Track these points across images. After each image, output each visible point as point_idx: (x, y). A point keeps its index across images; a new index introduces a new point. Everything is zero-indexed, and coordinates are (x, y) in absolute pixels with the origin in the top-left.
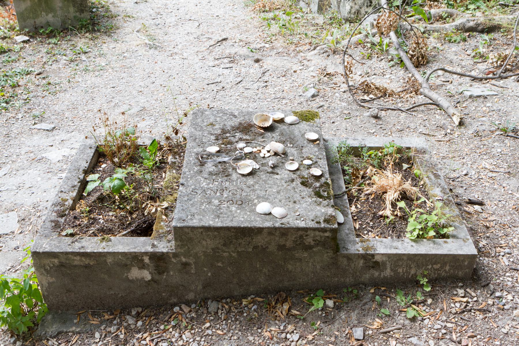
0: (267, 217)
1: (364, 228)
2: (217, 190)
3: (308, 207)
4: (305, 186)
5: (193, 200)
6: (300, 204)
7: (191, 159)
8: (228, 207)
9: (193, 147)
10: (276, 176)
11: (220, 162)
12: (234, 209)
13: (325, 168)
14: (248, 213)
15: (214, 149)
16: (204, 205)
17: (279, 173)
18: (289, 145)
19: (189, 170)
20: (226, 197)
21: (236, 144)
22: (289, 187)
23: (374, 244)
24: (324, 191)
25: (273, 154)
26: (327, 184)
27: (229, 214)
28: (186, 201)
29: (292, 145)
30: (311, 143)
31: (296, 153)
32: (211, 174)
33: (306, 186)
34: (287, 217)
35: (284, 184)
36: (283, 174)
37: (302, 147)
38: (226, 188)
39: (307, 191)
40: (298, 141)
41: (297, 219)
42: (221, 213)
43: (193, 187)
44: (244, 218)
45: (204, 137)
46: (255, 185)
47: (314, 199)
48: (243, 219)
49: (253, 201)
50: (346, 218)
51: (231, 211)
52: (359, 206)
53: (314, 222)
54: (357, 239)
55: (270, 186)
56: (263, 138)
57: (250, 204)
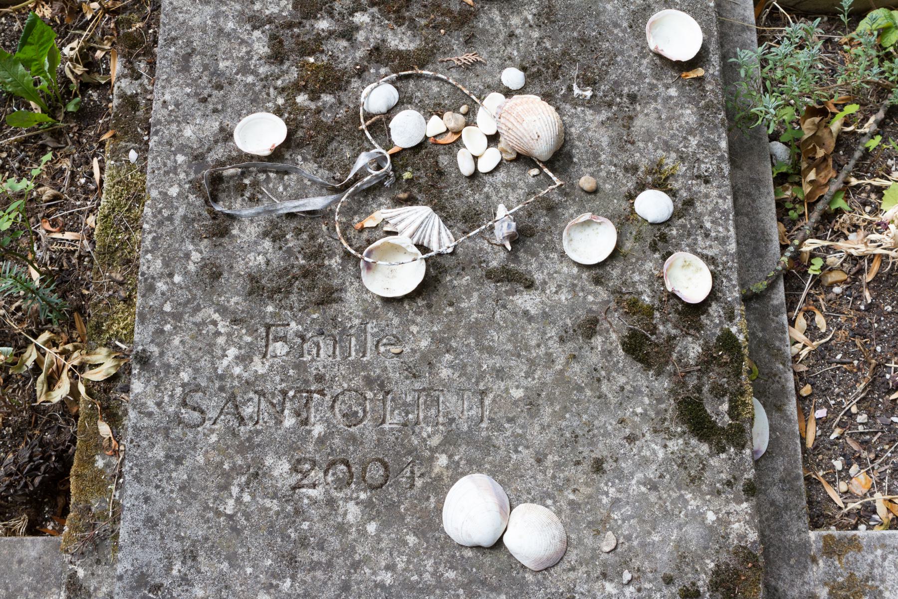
0: (487, 560)
1: (833, 443)
2: (284, 393)
3: (653, 497)
4: (641, 361)
5: (187, 463)
6: (620, 475)
7: (174, 191)
8: (331, 502)
9: (180, 117)
10: (527, 301)
11: (291, 216)
12: (353, 512)
13: (723, 241)
14: (411, 539)
15: (260, 133)
16: (235, 490)
17: (538, 277)
18: (576, 91)
19: (166, 264)
20: (321, 441)
21: (355, 83)
22: (576, 367)
23: (872, 566)
24: (718, 392)
25: (514, 156)
26: (728, 341)
27: (334, 543)
28: (159, 465)
29: (589, 93)
30: (670, 76)
31: (605, 141)
32: (256, 287)
33: (646, 362)
34: (565, 565)
35: (554, 346)
36: (548, 296)
37: (633, 98)
38: (320, 378)
39: (650, 390)
40: (612, 62)
41: (604, 575)
42: (303, 542)
43: (185, 376)
44: (390, 567)
45: (224, 45)
46: (438, 354)
47: (675, 445)
48: (387, 578)
49: (432, 459)
50: (776, 415)
51: (342, 529)
52: (820, 321)
53: (674, 590)
54: (813, 535)
55: (497, 361)
56: (469, 41)
57: (419, 483)
